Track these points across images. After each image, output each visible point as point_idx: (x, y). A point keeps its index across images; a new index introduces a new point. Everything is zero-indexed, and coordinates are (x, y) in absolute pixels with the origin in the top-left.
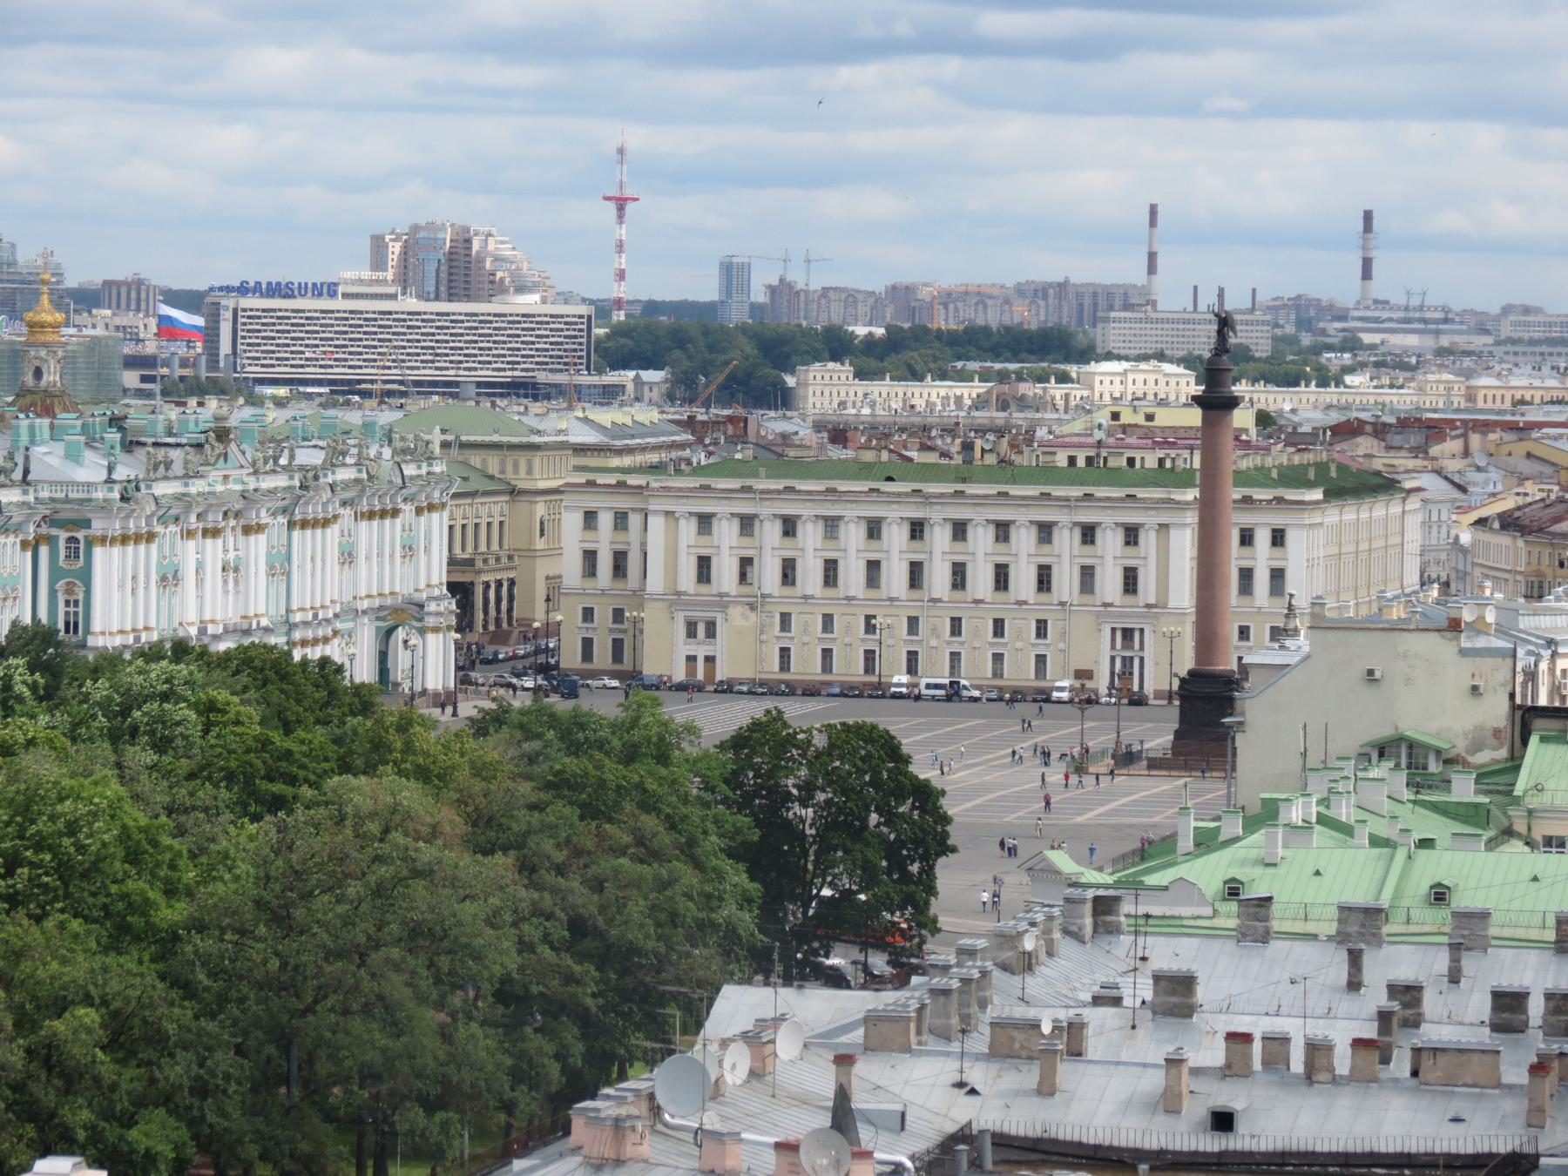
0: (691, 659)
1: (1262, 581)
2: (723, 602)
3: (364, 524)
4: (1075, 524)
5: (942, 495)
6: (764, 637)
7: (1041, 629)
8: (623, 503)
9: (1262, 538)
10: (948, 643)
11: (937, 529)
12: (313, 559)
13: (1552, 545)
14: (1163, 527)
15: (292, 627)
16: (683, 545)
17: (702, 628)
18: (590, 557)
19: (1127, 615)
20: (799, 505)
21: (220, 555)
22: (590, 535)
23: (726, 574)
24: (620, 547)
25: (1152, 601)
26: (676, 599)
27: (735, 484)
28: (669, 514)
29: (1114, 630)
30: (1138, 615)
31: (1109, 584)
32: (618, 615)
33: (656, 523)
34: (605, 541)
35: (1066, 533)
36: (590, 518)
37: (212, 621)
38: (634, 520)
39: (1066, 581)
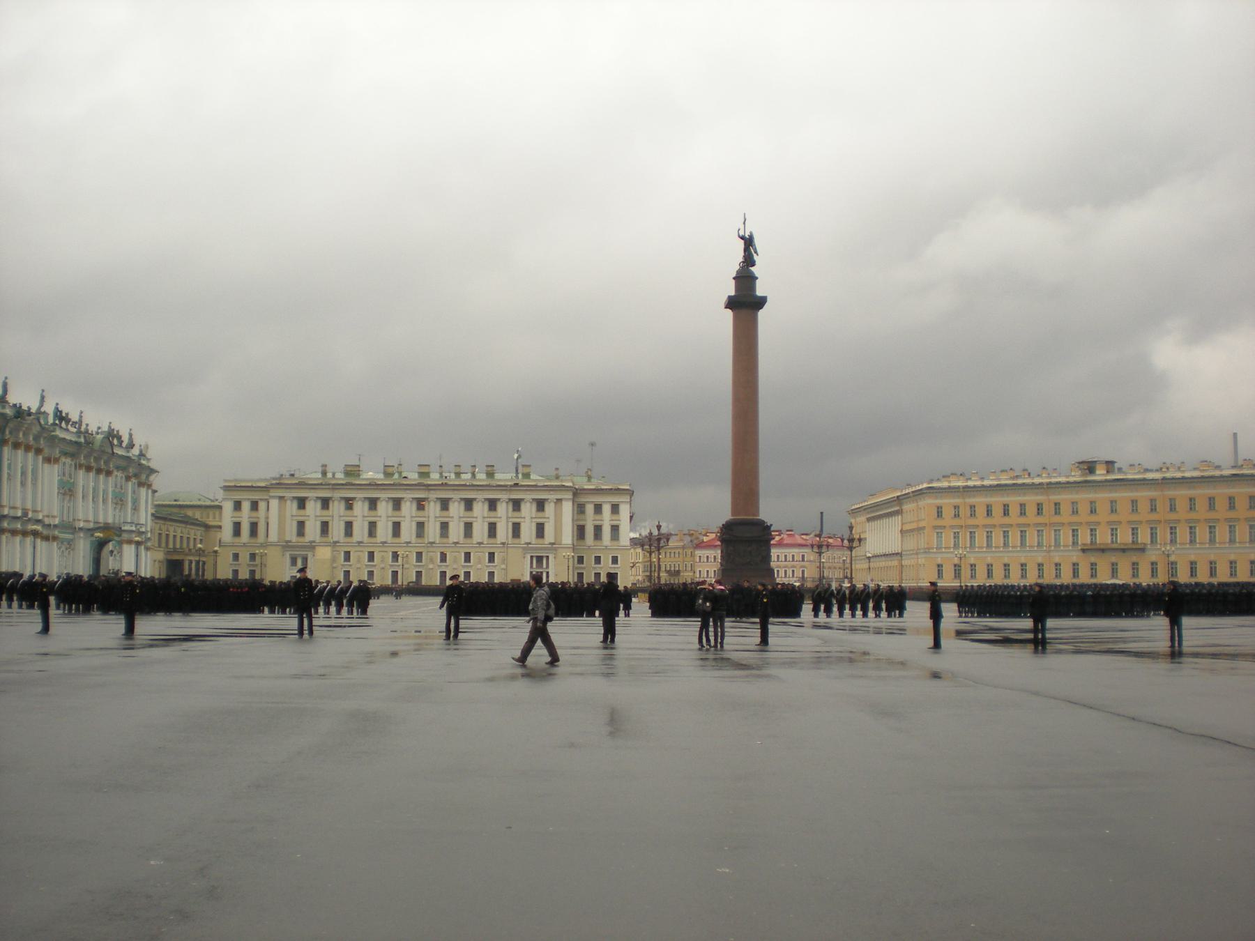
1: (606, 531)
2: (312, 546)
3: (81, 473)
7: (492, 557)
8: (255, 496)
9: (607, 509)
11: (432, 504)
12: (24, 474)
14: (559, 501)
16: (288, 514)
18: (237, 528)
22: (237, 514)
23: (312, 531)
26: (287, 546)
28: (281, 498)
31: (528, 532)
32: (253, 556)
33: (274, 504)
34: (245, 516)
36: (238, 506)
38: (262, 505)
39: (503, 532)
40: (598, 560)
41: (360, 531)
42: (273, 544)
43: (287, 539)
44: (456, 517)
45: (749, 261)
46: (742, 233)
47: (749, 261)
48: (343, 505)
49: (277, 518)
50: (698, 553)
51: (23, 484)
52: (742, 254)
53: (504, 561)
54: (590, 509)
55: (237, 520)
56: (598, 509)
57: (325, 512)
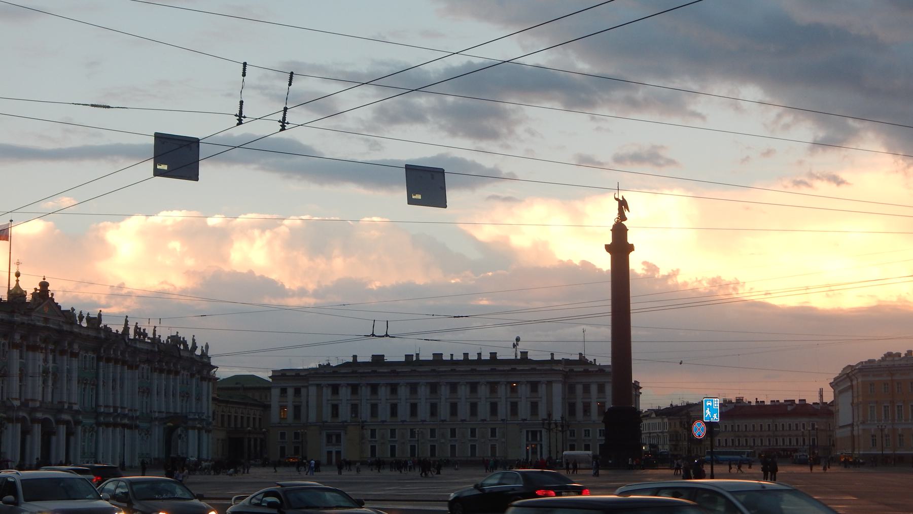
3: (156, 375)
4: (508, 383)
8: (298, 384)
9: (594, 389)
12: (114, 380)
14: (549, 383)
15: (97, 414)
17: (334, 437)
21: (41, 363)
23: (345, 413)
28: (318, 385)
29: (527, 432)
31: (524, 410)
32: (297, 435)
35: (503, 387)
36: (284, 391)
37: (32, 400)
38: (303, 391)
39: (503, 410)
40: (587, 433)
47: (622, 217)
51: (114, 388)
54: (579, 389)
56: (586, 388)
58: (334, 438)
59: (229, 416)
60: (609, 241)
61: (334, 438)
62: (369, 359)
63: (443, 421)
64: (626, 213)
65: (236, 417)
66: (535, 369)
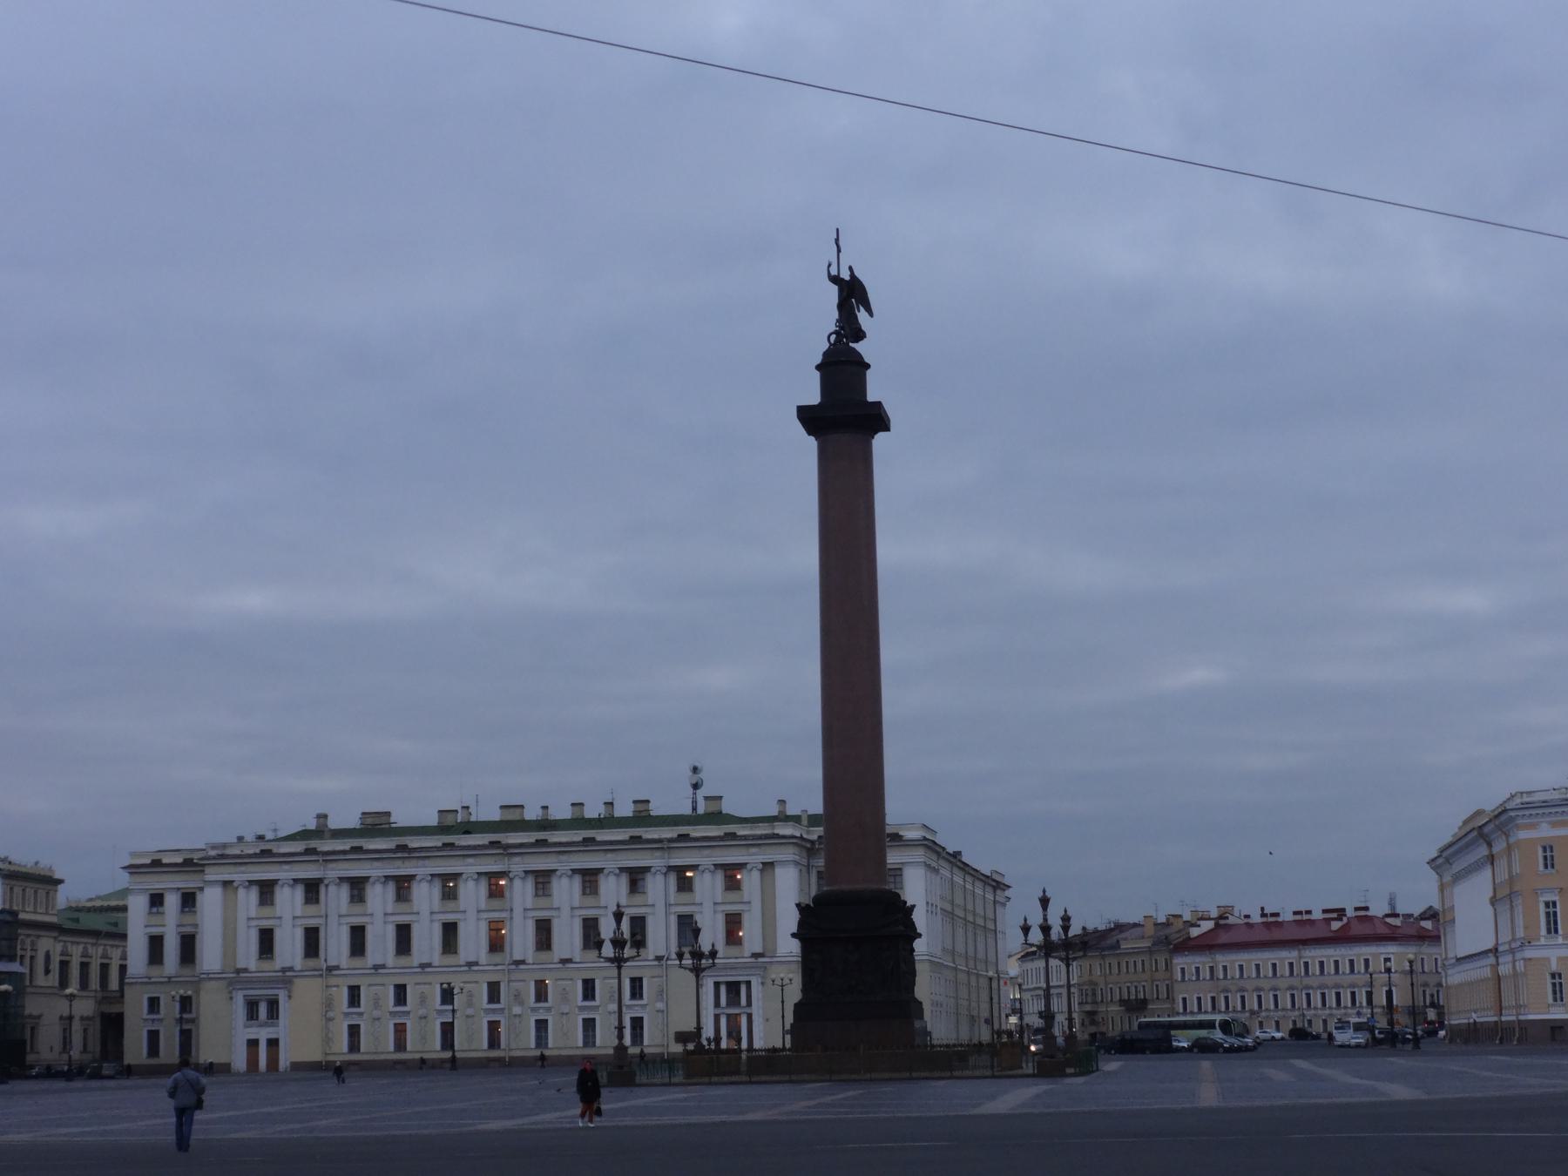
0: (253, 1044)
2: (286, 978)
4: (670, 868)
5: (521, 845)
6: (330, 1014)
10: (534, 1010)
13: (1103, 957)
14: (768, 866)
17: (264, 1008)
18: (156, 943)
19: (733, 967)
20: (367, 865)
23: (289, 947)
24: (188, 930)
25: (759, 950)
26: (236, 978)
27: (298, 847)
29: (717, 985)
30: (745, 966)
32: (186, 1003)
34: (170, 923)
35: (660, 878)
36: (157, 900)
41: (381, 943)
42: (209, 977)
43: (240, 965)
44: (566, 912)
45: (848, 330)
46: (834, 272)
47: (848, 330)
48: (345, 891)
49: (223, 924)
50: (1180, 961)
52: (836, 315)
53: (661, 994)
55: (155, 931)
57: (312, 909)
58: (263, 1010)
59: (105, 968)
60: (813, 397)
61: (263, 1010)
62: (353, 822)
63: (518, 963)
64: (862, 315)
65: (84, 966)
66: (733, 836)
